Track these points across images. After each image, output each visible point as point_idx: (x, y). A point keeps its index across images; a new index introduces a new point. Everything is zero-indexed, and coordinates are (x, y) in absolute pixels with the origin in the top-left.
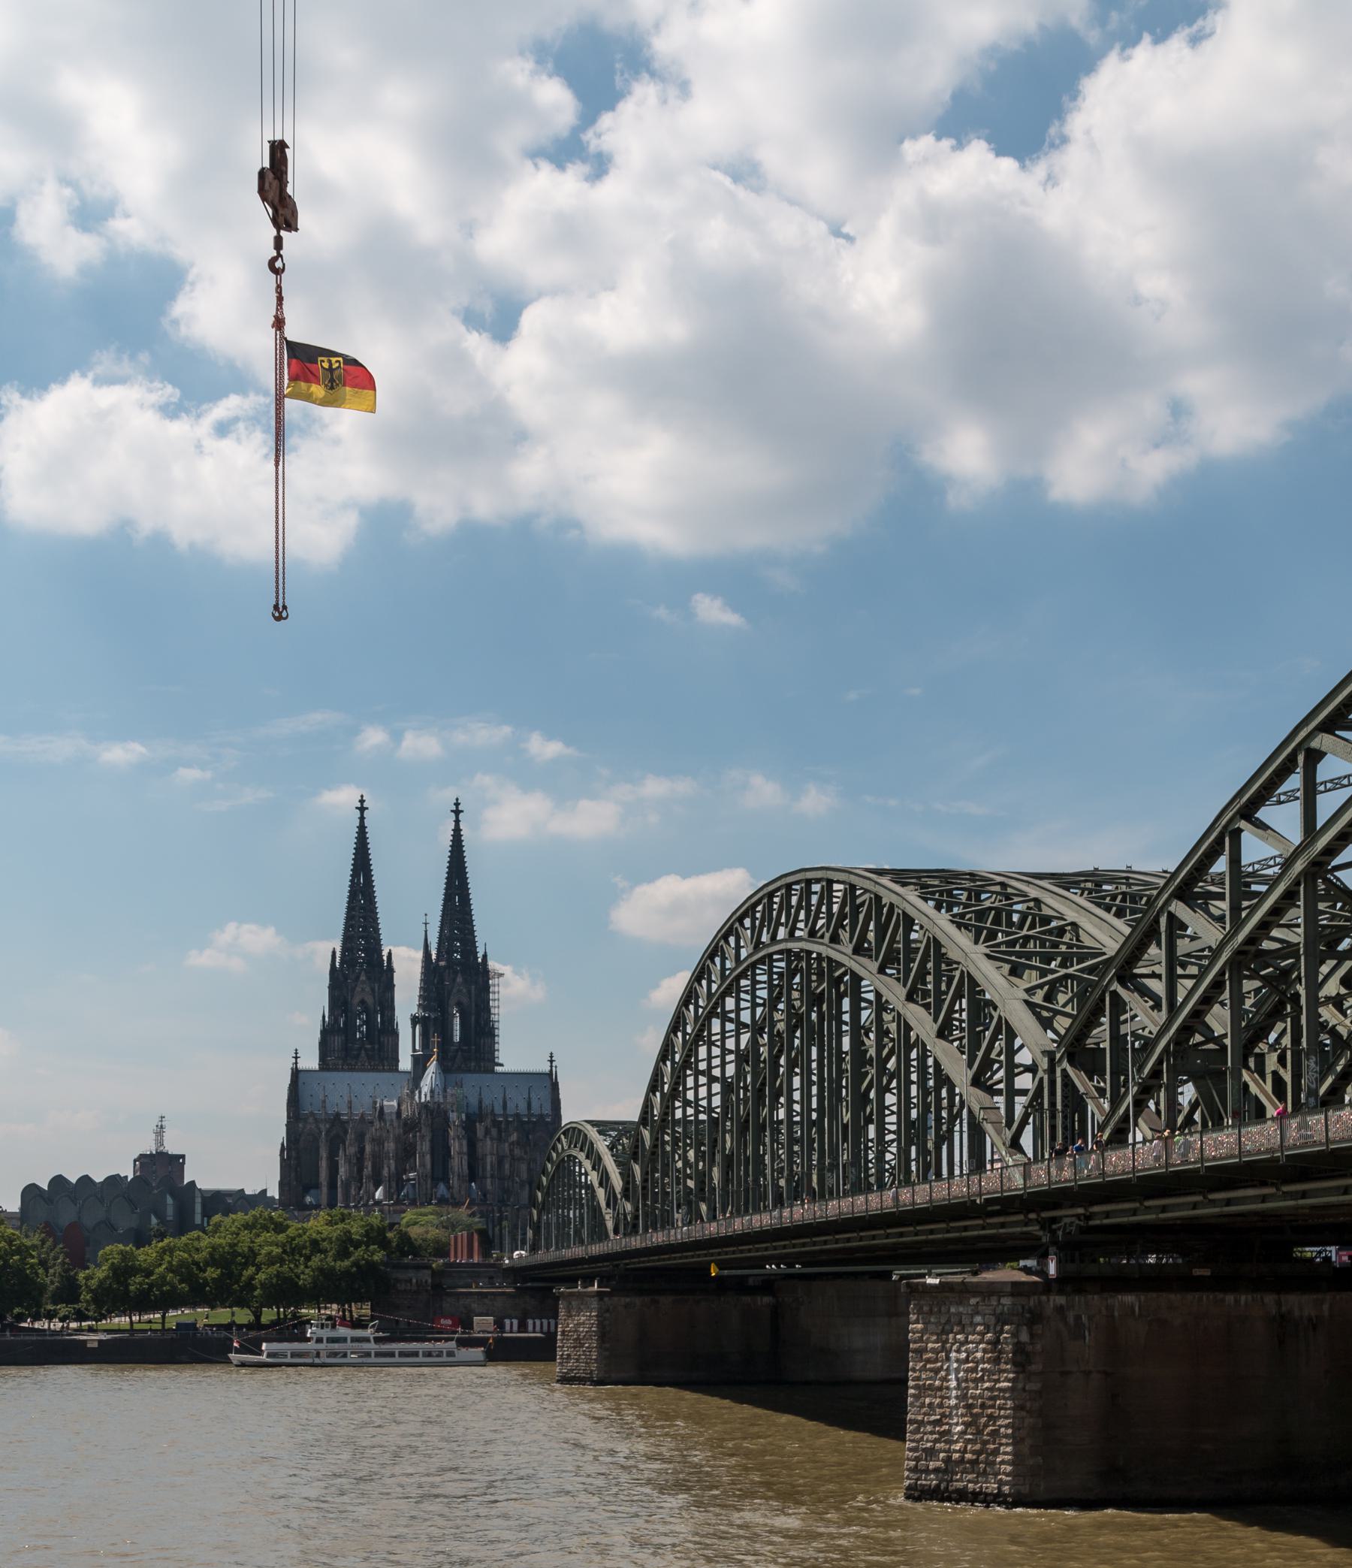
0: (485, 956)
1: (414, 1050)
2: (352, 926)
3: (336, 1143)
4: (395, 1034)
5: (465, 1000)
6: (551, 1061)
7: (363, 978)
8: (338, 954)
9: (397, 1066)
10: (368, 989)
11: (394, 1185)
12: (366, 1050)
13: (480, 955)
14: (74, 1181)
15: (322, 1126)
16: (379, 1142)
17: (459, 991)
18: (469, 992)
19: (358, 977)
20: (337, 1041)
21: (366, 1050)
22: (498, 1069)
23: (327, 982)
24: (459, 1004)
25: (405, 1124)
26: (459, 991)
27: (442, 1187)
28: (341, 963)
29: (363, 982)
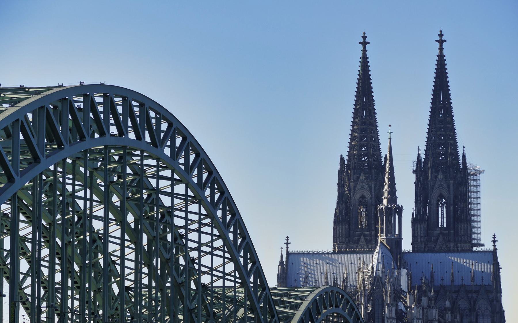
6: (494, 241)
7: (362, 178)
10: (366, 187)
12: (365, 236)
17: (441, 186)
18: (448, 186)
19: (358, 178)
20: (342, 229)
21: (365, 236)
22: (475, 249)
26: (441, 186)
29: (362, 182)
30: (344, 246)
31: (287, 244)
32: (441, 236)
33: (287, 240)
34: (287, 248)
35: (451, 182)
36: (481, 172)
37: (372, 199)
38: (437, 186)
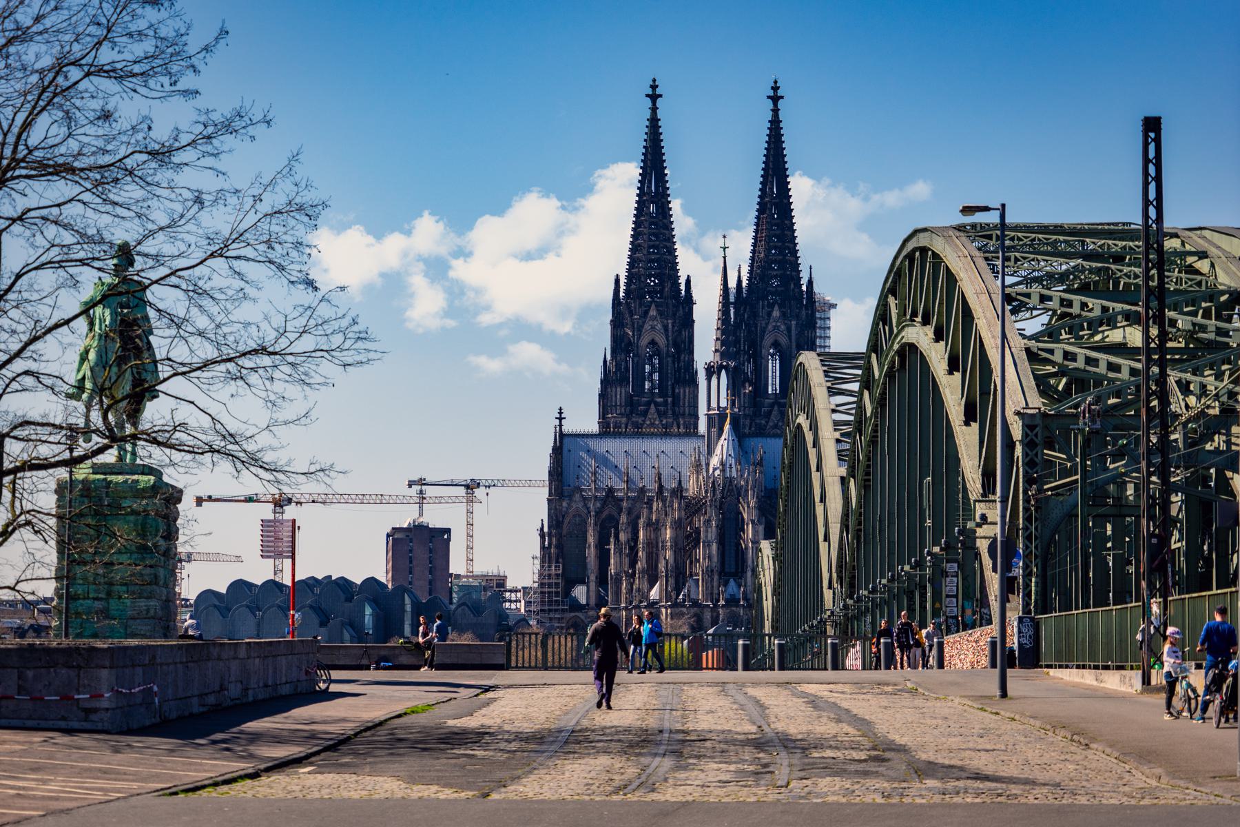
0: (810, 282)
1: (709, 408)
2: (639, 245)
3: (607, 528)
4: (693, 382)
5: (783, 340)
7: (653, 312)
8: (623, 281)
9: (696, 427)
10: (659, 326)
11: (672, 581)
12: (657, 404)
13: (804, 281)
14: (224, 592)
15: (591, 505)
16: (655, 527)
18: (789, 329)
19: (646, 313)
20: (619, 394)
21: (657, 404)
23: (610, 317)
24: (776, 344)
25: (688, 505)
27: (732, 582)
28: (626, 292)
29: (654, 318)
30: (624, 420)
31: (560, 419)
32: (776, 408)
33: (561, 413)
34: (561, 425)
35: (793, 323)
36: (834, 306)
37: (668, 346)
38: (770, 327)
